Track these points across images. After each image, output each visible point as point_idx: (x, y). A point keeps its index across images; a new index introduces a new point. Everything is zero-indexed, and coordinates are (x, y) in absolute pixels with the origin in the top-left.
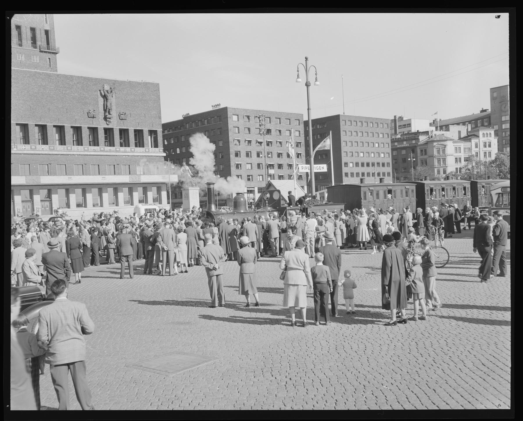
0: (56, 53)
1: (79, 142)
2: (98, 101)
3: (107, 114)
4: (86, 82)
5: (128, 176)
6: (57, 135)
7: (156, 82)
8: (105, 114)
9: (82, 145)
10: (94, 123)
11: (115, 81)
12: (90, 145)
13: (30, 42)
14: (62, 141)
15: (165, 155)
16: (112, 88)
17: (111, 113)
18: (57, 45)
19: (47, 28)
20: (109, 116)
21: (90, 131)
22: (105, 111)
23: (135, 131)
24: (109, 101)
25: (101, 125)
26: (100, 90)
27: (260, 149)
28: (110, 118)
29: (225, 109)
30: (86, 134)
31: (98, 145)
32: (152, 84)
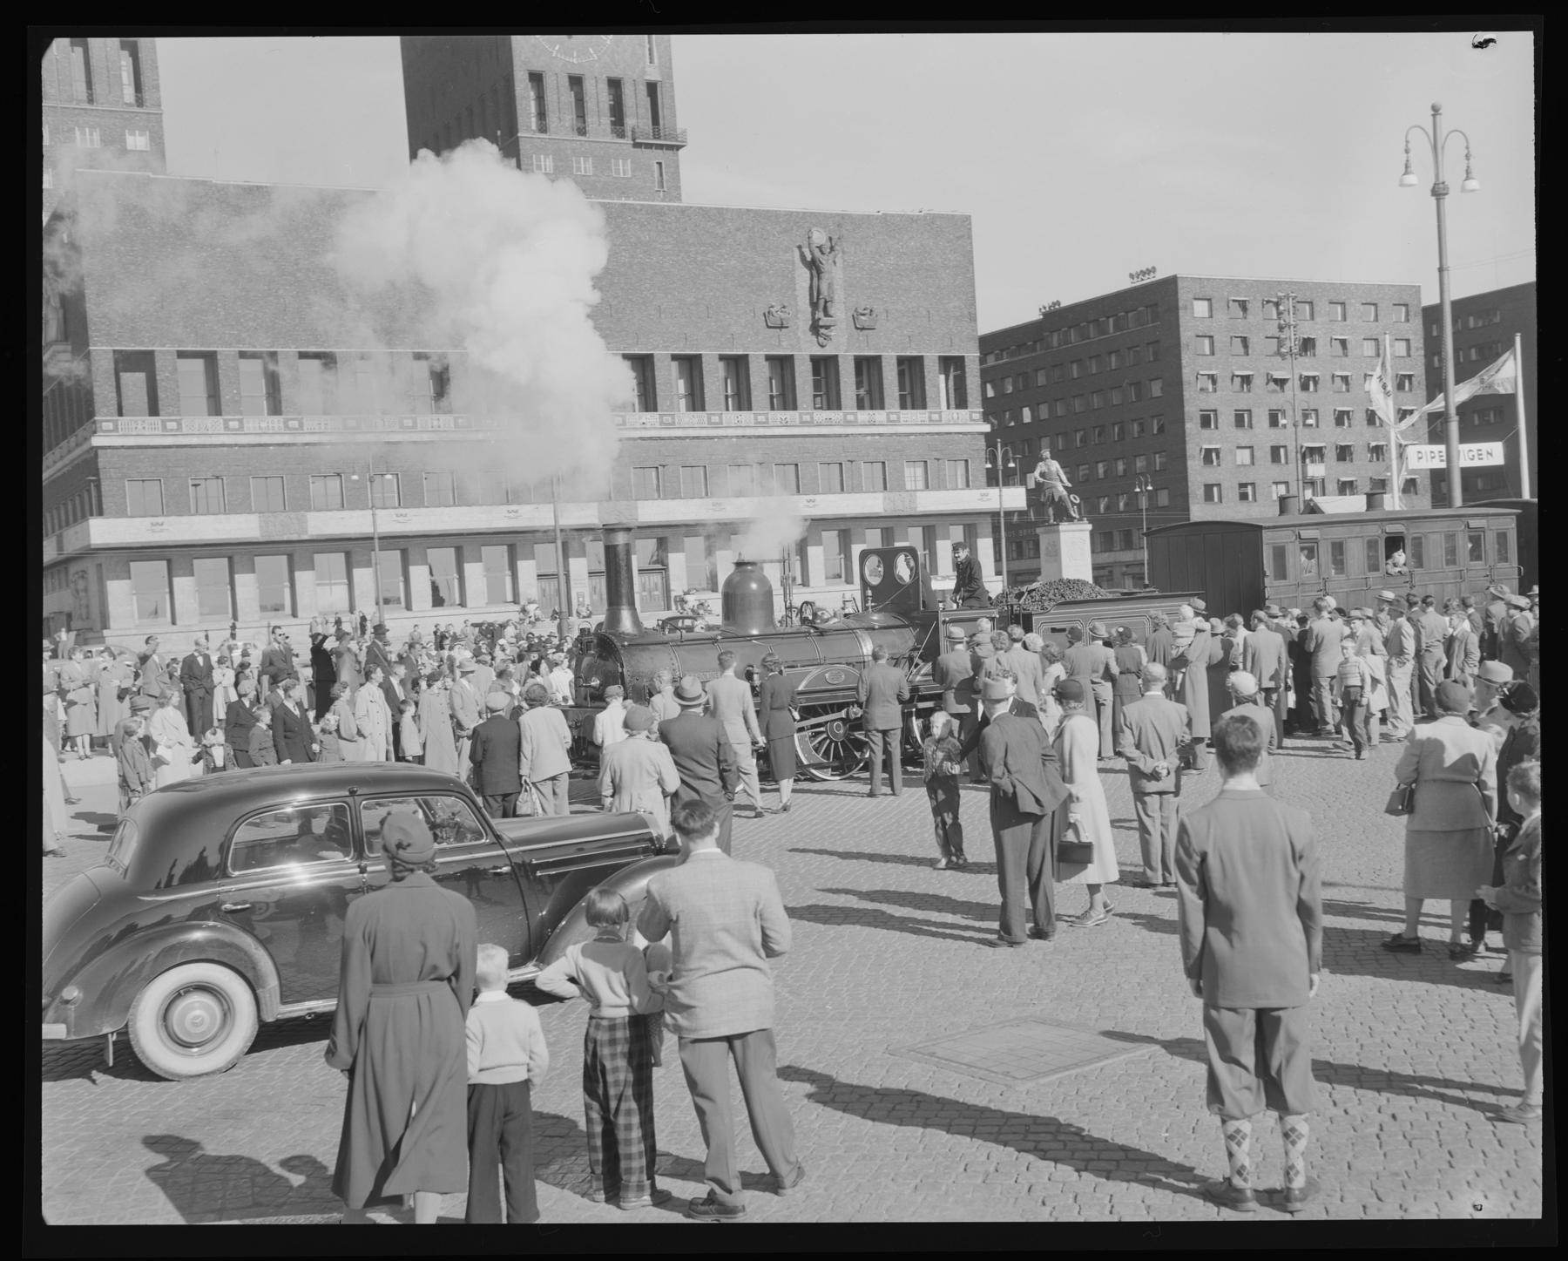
0: (678, 148)
1: (742, 400)
2: (793, 279)
3: (820, 314)
4: (760, 224)
5: (880, 496)
6: (681, 383)
7: (961, 211)
8: (813, 314)
9: (750, 409)
10: (784, 344)
11: (843, 216)
12: (772, 408)
13: (607, 120)
14: (696, 401)
15: (987, 428)
16: (835, 237)
17: (832, 311)
18: (680, 126)
19: (653, 75)
20: (824, 321)
21: (771, 367)
22: (814, 305)
23: (901, 361)
24: (825, 276)
25: (804, 348)
26: (800, 247)
27: (1278, 400)
28: (827, 327)
29: (1171, 283)
30: (760, 375)
31: (795, 408)
32: (950, 218)
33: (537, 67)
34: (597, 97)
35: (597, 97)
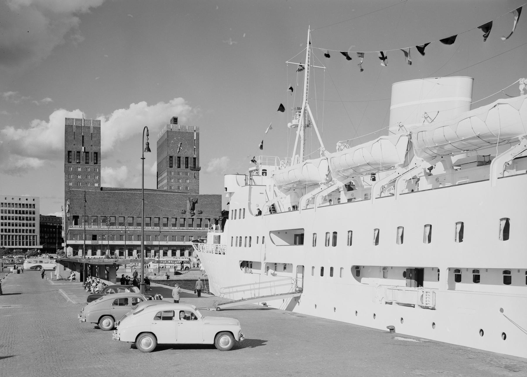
19: (195, 156)
34: (183, 160)
35: (183, 160)
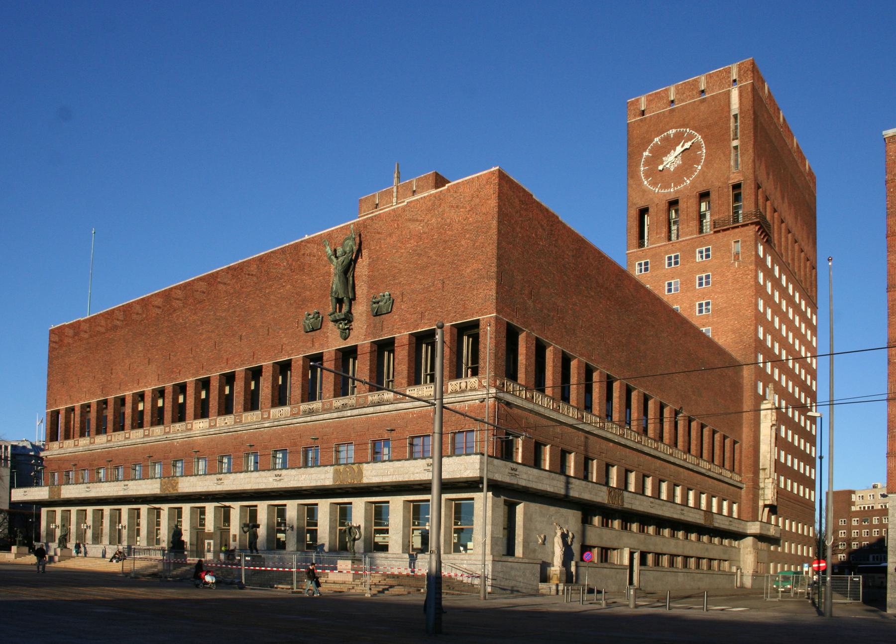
33: (642, 204)
